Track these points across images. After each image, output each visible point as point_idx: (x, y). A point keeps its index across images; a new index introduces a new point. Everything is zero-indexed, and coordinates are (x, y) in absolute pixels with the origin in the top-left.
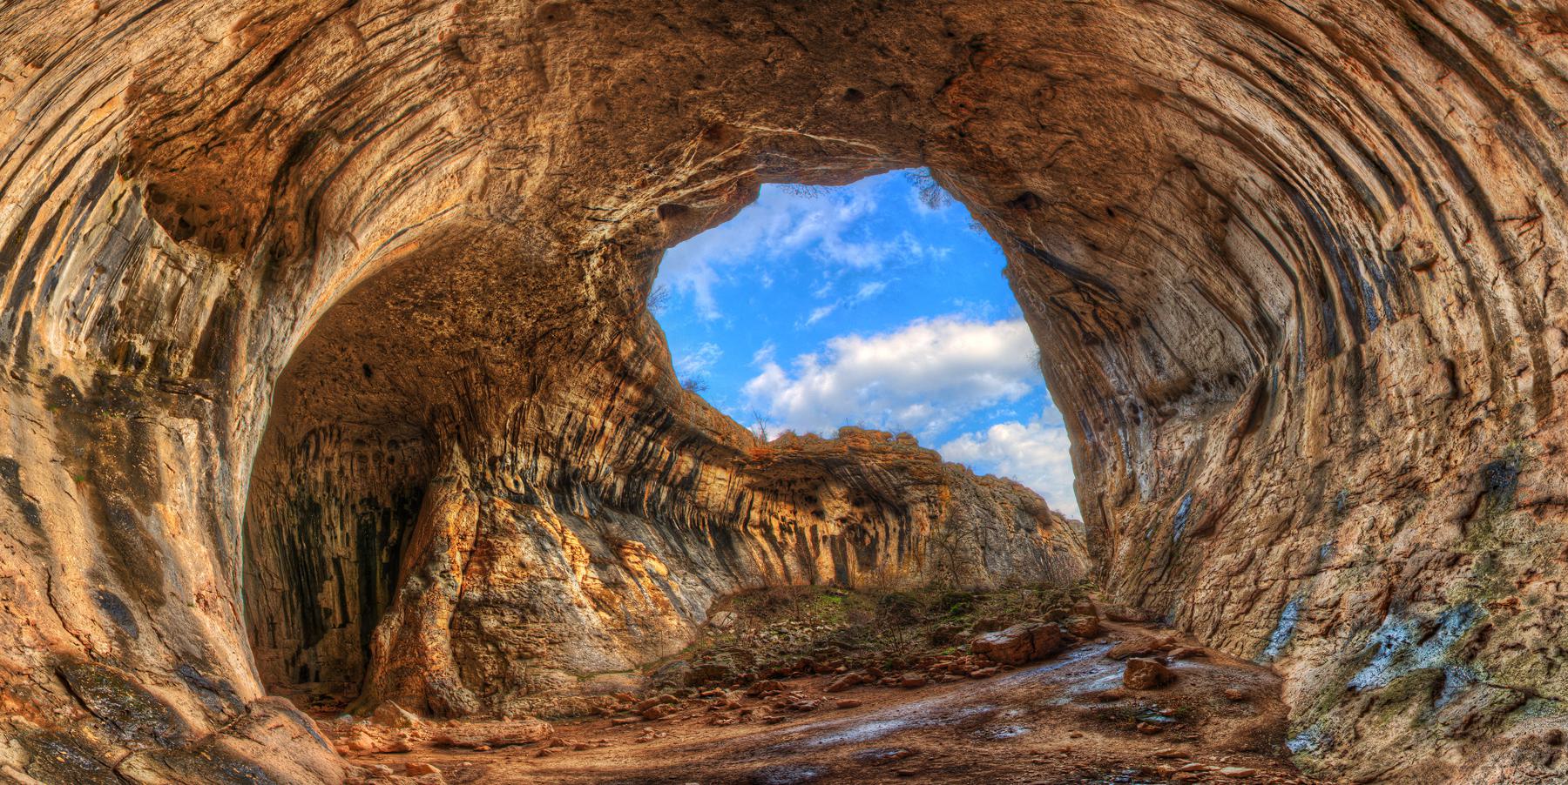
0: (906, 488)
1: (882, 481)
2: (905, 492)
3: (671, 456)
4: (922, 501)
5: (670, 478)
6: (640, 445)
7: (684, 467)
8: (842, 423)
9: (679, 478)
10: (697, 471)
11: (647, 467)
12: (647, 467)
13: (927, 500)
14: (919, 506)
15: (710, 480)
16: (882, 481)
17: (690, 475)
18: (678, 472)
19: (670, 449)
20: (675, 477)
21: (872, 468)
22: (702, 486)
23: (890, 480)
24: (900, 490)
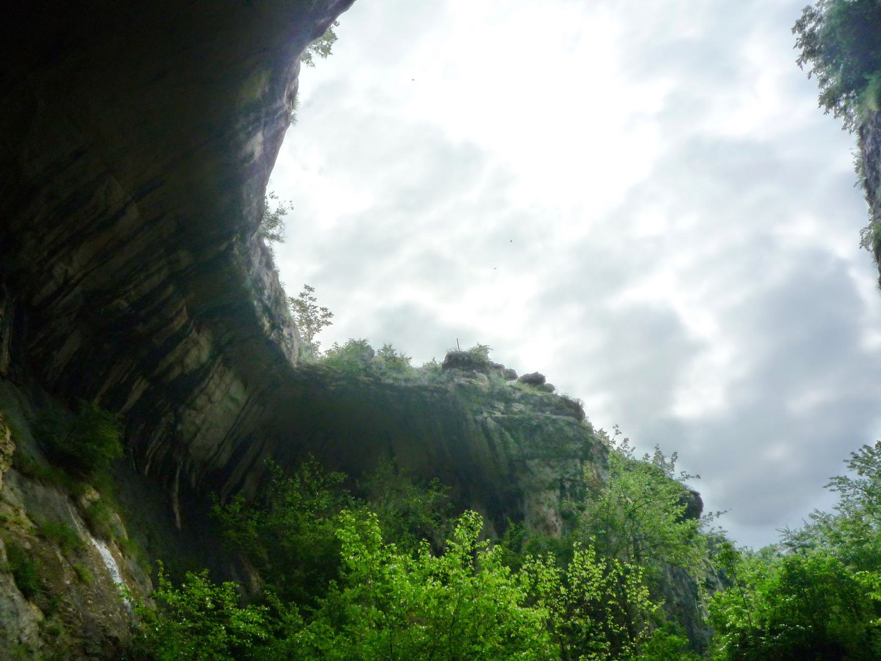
0: (530, 463)
2: (526, 469)
3: (186, 326)
4: (552, 487)
5: (163, 365)
6: (156, 280)
7: (194, 353)
8: (452, 347)
9: (177, 371)
10: (208, 371)
11: (140, 328)
12: (140, 328)
13: (559, 485)
15: (218, 395)
16: (492, 446)
18: (181, 362)
19: (191, 313)
20: (170, 368)
21: (483, 424)
22: (200, 401)
23: (505, 444)
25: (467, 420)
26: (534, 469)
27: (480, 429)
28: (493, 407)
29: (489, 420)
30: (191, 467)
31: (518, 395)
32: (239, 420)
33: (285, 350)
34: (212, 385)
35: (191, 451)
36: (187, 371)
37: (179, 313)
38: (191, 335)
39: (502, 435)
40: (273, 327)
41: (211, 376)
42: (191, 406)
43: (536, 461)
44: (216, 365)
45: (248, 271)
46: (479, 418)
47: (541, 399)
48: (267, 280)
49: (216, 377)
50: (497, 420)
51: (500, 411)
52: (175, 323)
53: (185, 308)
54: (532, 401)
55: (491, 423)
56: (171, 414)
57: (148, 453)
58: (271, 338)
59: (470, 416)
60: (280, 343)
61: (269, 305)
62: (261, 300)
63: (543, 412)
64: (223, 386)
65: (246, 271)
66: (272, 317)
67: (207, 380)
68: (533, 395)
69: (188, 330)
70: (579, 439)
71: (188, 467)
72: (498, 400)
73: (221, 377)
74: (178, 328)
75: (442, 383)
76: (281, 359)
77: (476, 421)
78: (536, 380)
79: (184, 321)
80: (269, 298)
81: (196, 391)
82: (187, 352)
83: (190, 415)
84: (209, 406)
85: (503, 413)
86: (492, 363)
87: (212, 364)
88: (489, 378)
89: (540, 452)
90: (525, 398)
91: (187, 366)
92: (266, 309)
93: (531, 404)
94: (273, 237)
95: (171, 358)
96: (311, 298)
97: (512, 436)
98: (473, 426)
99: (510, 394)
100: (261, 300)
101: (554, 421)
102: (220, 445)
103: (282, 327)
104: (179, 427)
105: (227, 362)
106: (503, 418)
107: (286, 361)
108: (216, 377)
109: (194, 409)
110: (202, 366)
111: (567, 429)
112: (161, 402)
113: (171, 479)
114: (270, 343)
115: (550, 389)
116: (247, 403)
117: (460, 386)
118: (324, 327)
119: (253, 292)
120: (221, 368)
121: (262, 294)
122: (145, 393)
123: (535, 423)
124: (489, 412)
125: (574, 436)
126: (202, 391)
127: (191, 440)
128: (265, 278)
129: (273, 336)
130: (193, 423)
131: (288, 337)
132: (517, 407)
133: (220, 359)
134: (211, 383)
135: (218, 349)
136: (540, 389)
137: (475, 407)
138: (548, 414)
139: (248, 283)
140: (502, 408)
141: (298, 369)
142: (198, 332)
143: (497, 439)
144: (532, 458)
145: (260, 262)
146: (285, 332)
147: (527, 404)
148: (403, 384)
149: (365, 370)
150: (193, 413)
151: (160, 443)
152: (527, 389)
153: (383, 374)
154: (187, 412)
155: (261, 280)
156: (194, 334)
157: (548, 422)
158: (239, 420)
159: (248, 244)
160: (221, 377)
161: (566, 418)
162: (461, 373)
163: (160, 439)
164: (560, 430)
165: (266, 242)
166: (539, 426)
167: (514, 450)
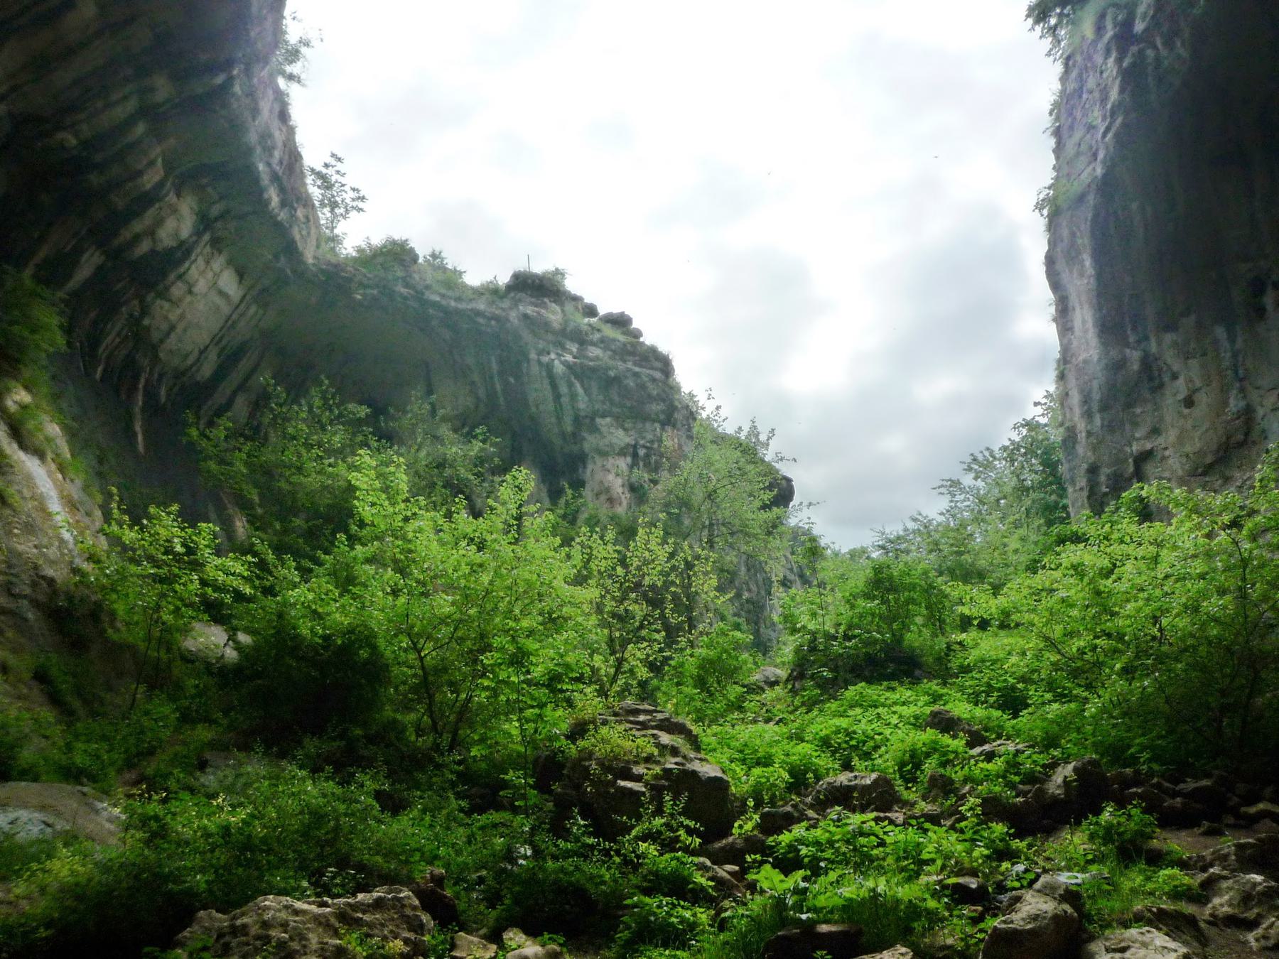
1: (557, 397)
2: (594, 429)
3: (161, 184)
4: (622, 453)
5: (126, 235)
7: (170, 224)
8: (521, 266)
9: (144, 247)
10: (188, 253)
11: (95, 179)
12: (95, 179)
13: (632, 452)
14: (610, 462)
15: (201, 286)
16: (557, 397)
17: (170, 252)
18: (151, 233)
19: (169, 167)
20: (137, 238)
21: (549, 367)
22: (177, 290)
23: (573, 396)
24: (585, 423)
25: (528, 361)
26: (604, 429)
27: (544, 374)
28: (564, 348)
29: (556, 362)
30: (161, 376)
31: (597, 336)
32: (230, 322)
33: (297, 237)
34: (194, 272)
35: (161, 355)
36: (159, 248)
37: (152, 163)
38: (167, 199)
39: (570, 385)
40: (283, 204)
41: (193, 258)
42: (164, 295)
43: (608, 419)
44: (203, 244)
45: (254, 120)
46: (545, 359)
47: (625, 345)
48: (279, 137)
49: (201, 261)
50: (565, 363)
51: (571, 353)
52: (146, 177)
53: (160, 160)
54: (613, 347)
55: (559, 368)
56: (136, 302)
57: (101, 350)
58: (279, 218)
59: (533, 356)
60: (291, 226)
61: (280, 174)
62: (269, 164)
63: (625, 361)
64: (210, 275)
65: (250, 119)
66: (282, 190)
67: (187, 265)
68: (614, 340)
69: (164, 192)
70: (663, 400)
71: (156, 376)
72: (572, 340)
73: (208, 262)
74: (148, 186)
75: (503, 309)
76: (291, 249)
77: (539, 362)
78: (620, 322)
79: (156, 179)
80: (281, 162)
81: (172, 277)
82: (159, 222)
83: (162, 308)
84: (189, 298)
85: (575, 357)
86: (569, 292)
87: (196, 242)
88: (563, 311)
89: (615, 410)
90: (604, 343)
91: (161, 241)
92: (275, 178)
93: (612, 350)
94: (291, 77)
95: (138, 226)
96: (338, 172)
97: (582, 386)
98: (535, 369)
99: (586, 334)
100: (269, 164)
101: (636, 375)
102: (201, 352)
103: (295, 205)
104: (146, 322)
105: (216, 243)
106: (575, 363)
107: (297, 252)
108: (201, 261)
109: (170, 300)
110: (182, 243)
111: (650, 386)
112: (119, 286)
113: (133, 389)
114: (278, 225)
115: (637, 334)
116: (241, 301)
117: (526, 316)
118: (353, 214)
119: (258, 150)
120: (208, 249)
121: (271, 155)
122: (100, 269)
123: (612, 373)
124: (557, 354)
125: (658, 395)
126: (180, 277)
127: (162, 341)
128: (277, 134)
129: (283, 216)
130: (166, 318)
131: (303, 219)
132: (594, 352)
133: (207, 237)
134: (193, 267)
135: (205, 222)
136: (624, 333)
137: (541, 345)
138: (630, 365)
139: (252, 137)
140: (575, 350)
141: (314, 265)
142: (178, 195)
143: (564, 389)
144: (603, 416)
145: (271, 111)
146: (300, 213)
147: (605, 349)
148: (453, 304)
149: (404, 279)
150: (166, 305)
151: (118, 340)
152: (609, 332)
153: (428, 287)
154: (158, 302)
155: (270, 136)
156: (172, 198)
157: (628, 374)
158: (230, 322)
159: (255, 80)
160: (208, 262)
161: (651, 372)
162: (529, 299)
163: (118, 334)
164: (643, 387)
165: (281, 82)
166: (617, 380)
167: (582, 404)
